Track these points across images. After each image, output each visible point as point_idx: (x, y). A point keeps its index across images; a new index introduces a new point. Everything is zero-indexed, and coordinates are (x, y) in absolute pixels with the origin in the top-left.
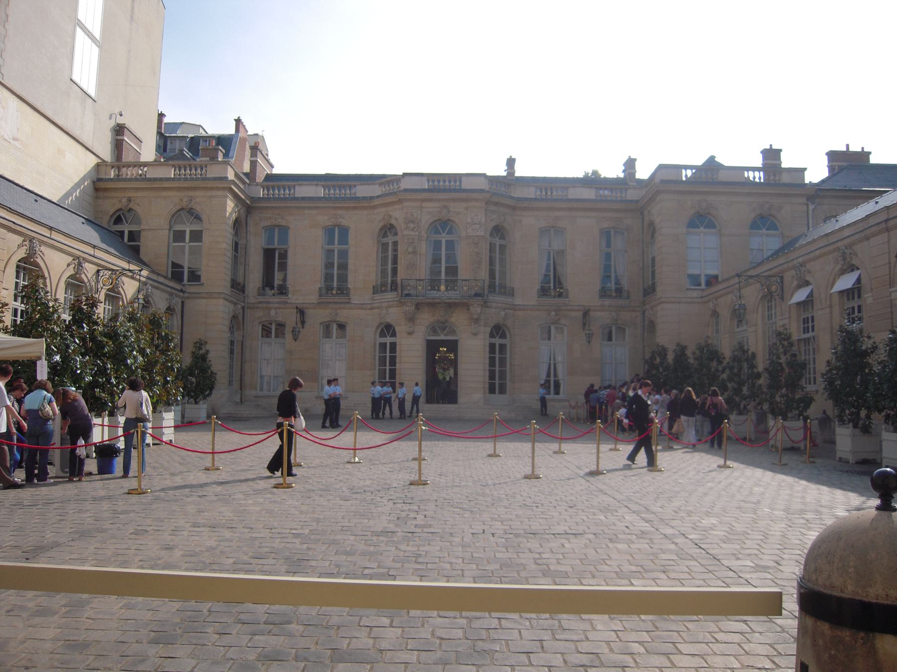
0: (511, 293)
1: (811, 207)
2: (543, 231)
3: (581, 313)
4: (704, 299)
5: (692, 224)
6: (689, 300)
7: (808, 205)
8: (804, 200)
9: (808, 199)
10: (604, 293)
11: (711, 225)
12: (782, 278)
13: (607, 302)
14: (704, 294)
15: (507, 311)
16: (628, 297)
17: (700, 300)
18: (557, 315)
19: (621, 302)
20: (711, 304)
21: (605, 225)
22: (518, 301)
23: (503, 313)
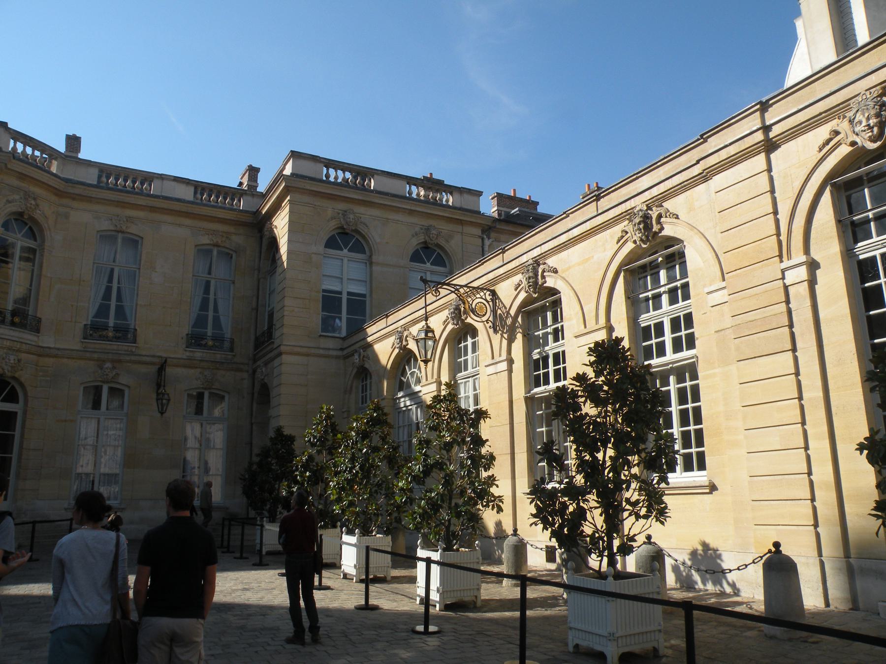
0: (36, 327)
1: (487, 242)
2: (108, 237)
3: (154, 369)
4: (345, 352)
5: (331, 243)
6: (321, 352)
7: (483, 239)
8: (478, 231)
9: (483, 232)
10: (195, 340)
11: (358, 248)
12: (494, 293)
13: (199, 354)
14: (345, 345)
15: (23, 356)
16: (232, 349)
17: (339, 353)
18: (114, 368)
19: (219, 356)
20: (356, 356)
21: (205, 240)
22: (47, 340)
23: (12, 358)
